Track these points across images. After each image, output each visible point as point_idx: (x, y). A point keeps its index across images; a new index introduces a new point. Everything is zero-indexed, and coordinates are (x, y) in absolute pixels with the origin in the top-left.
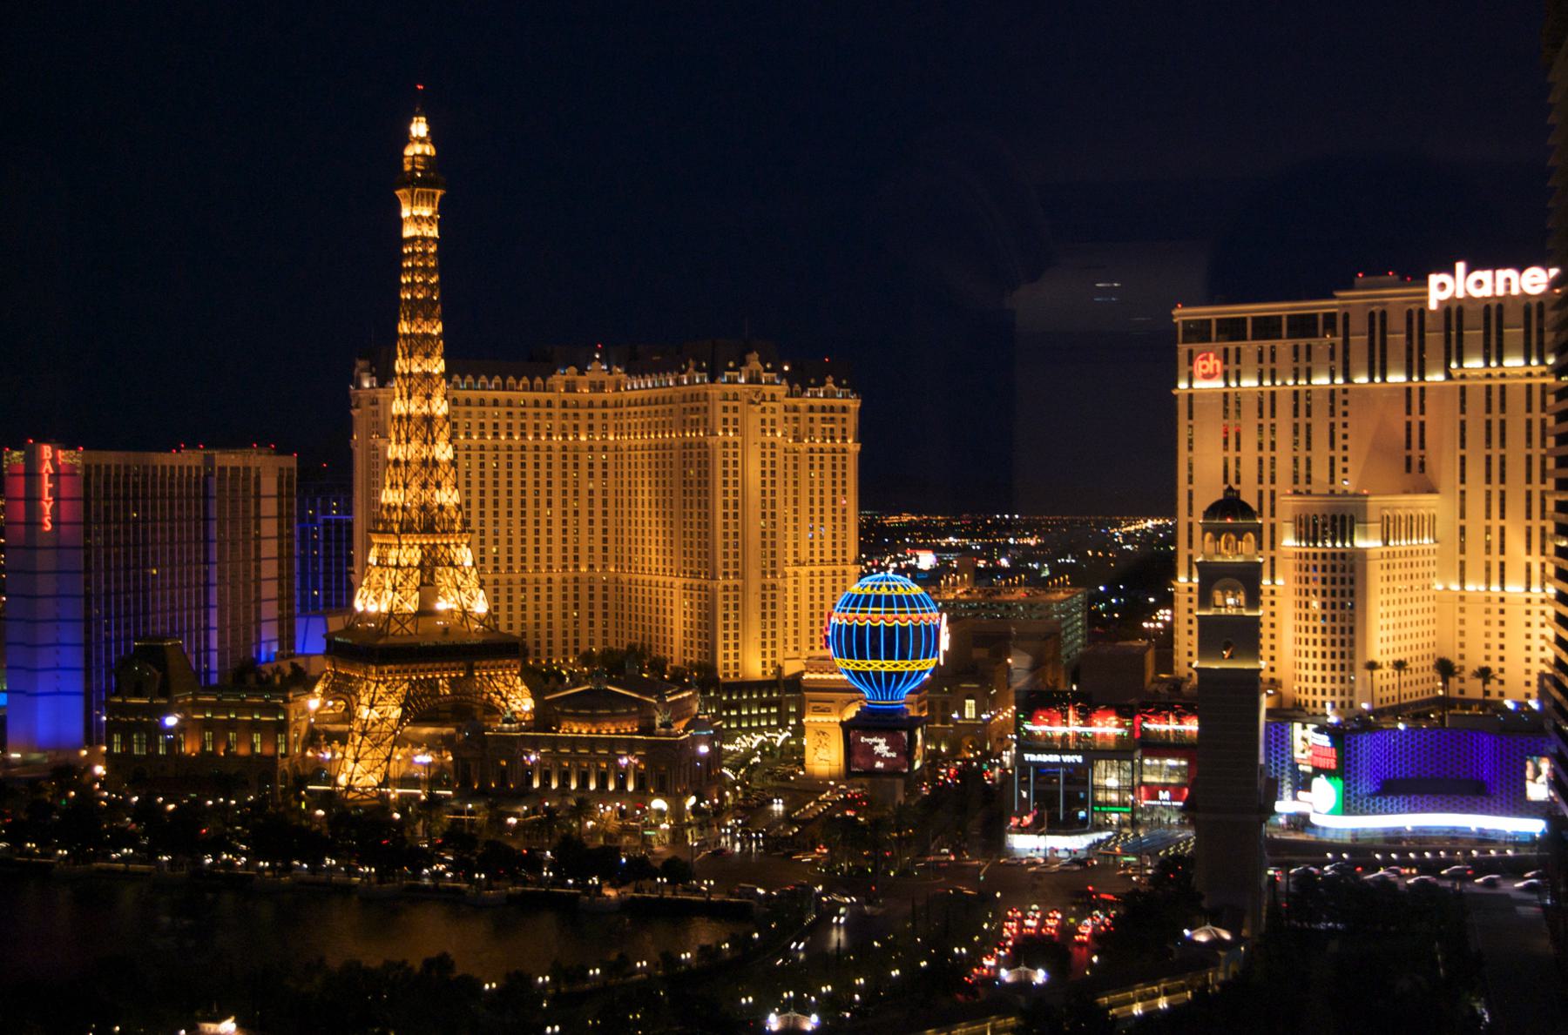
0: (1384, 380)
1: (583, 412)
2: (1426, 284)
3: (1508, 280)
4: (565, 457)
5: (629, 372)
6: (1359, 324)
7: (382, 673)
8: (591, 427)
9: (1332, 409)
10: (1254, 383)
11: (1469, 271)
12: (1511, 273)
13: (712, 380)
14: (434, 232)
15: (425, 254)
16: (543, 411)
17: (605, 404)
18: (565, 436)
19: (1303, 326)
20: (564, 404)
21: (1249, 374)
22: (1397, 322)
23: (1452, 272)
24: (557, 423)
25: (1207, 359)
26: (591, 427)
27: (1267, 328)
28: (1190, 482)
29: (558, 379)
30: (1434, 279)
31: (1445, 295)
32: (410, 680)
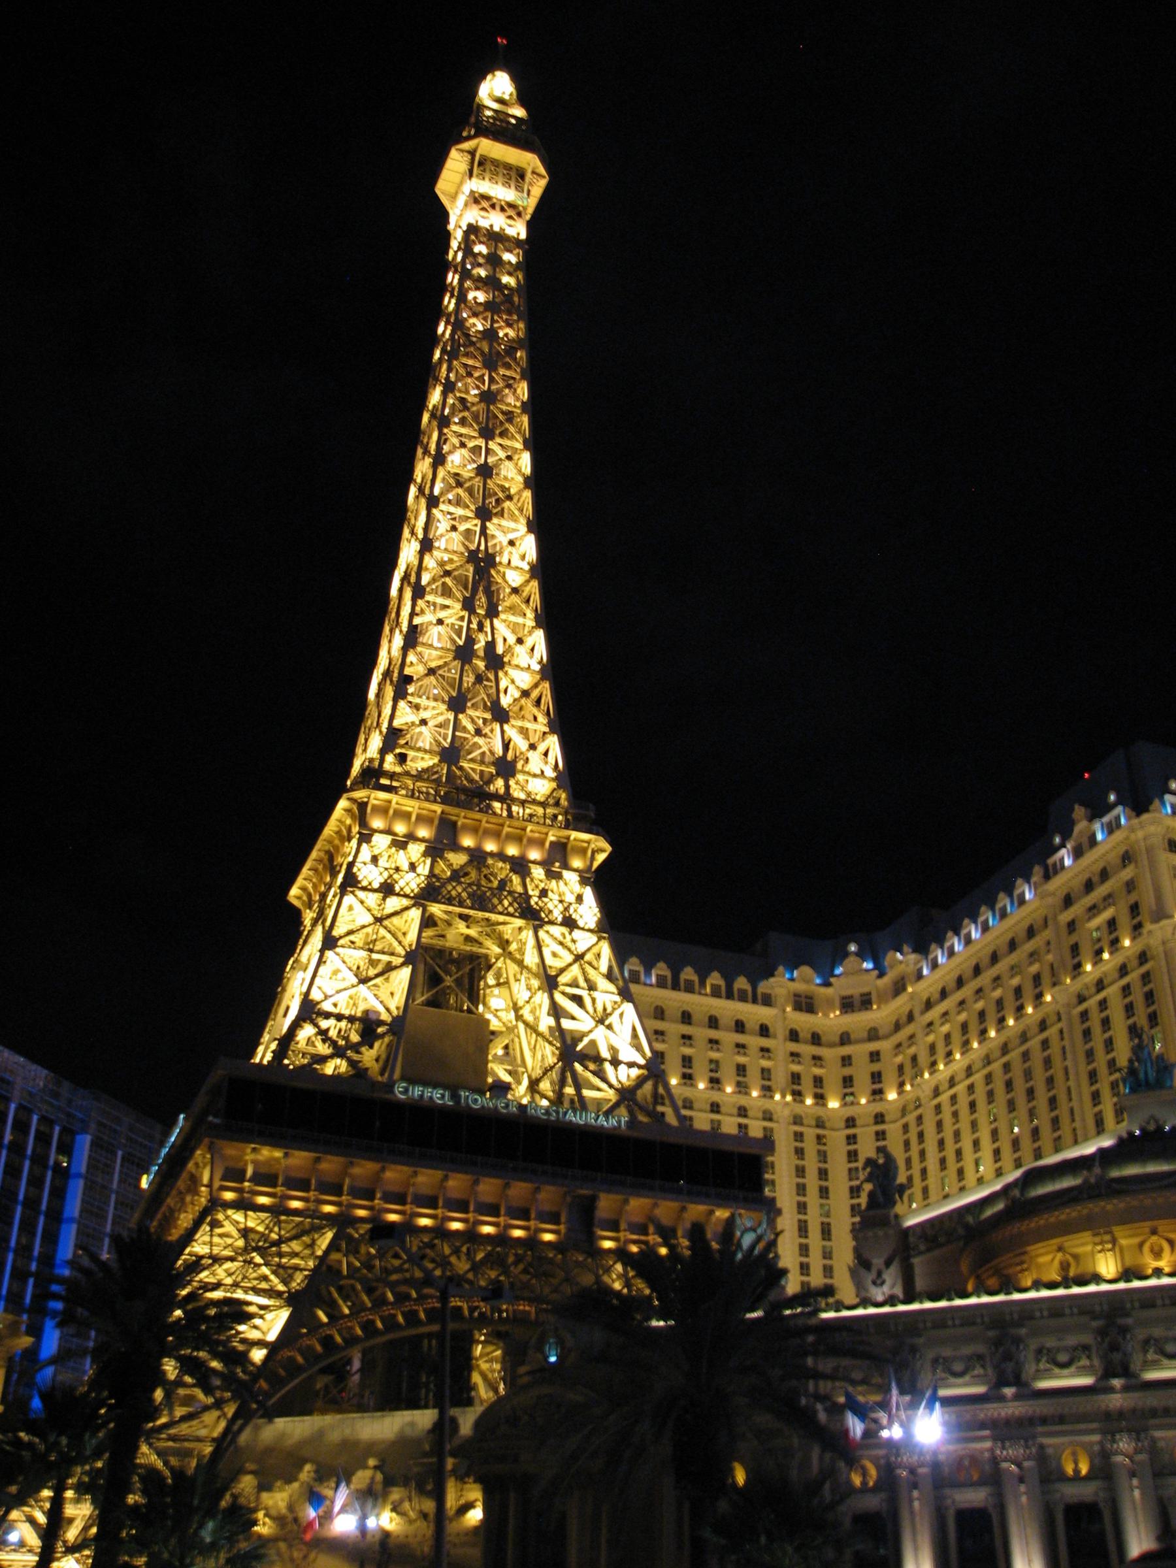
1: (831, 1054)
4: (799, 1136)
5: (922, 949)
7: (235, 1174)
8: (848, 1081)
13: (1140, 807)
14: (519, 230)
15: (494, 260)
16: (754, 1042)
17: (873, 1035)
18: (798, 1095)
20: (794, 1036)
24: (781, 1070)
26: (848, 1081)
29: (782, 983)
32: (342, 1222)
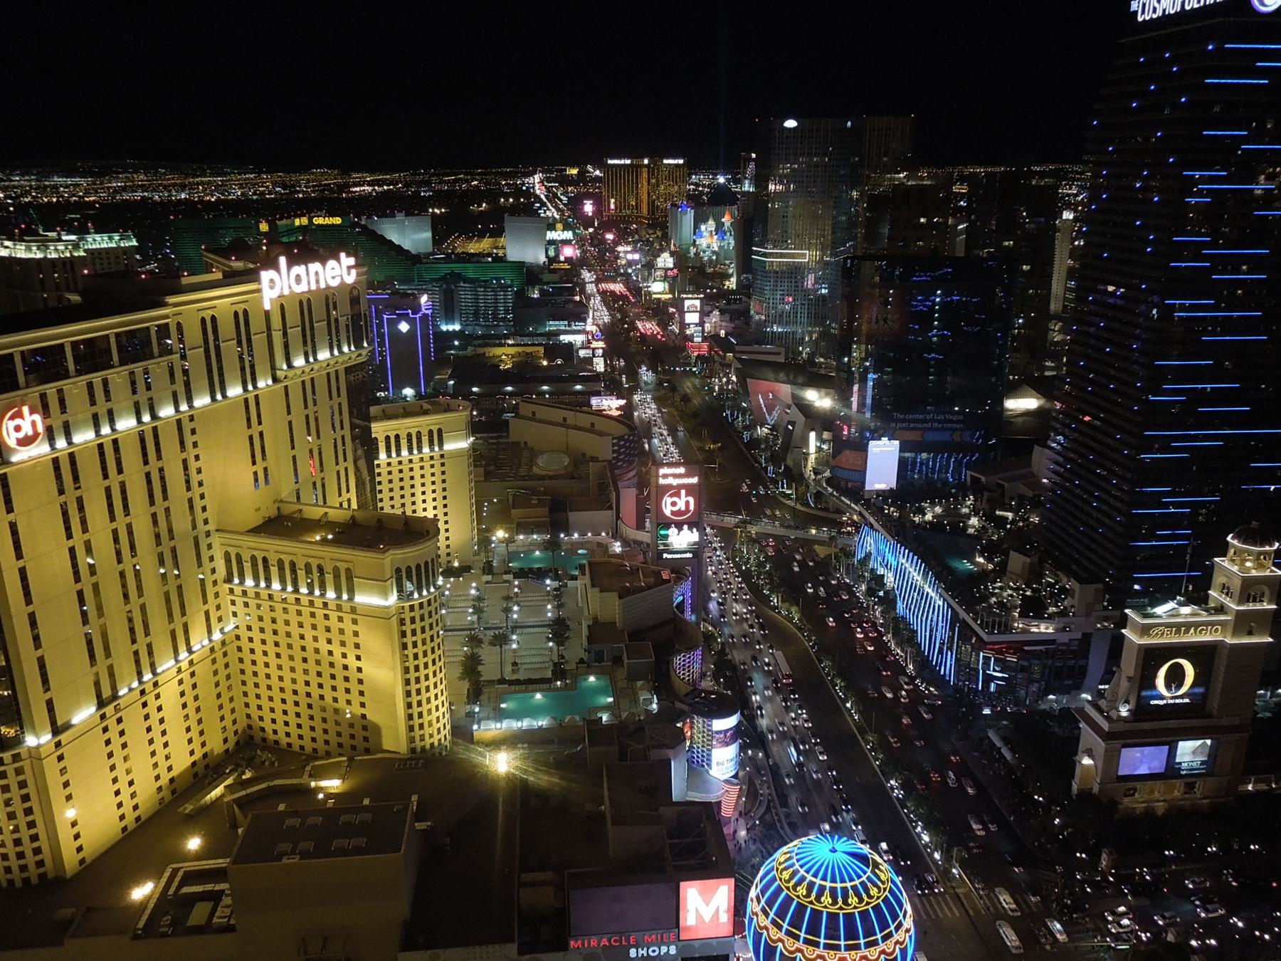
0: (224, 396)
2: (257, 280)
3: (317, 273)
6: (193, 334)
9: (182, 443)
10: (89, 435)
11: (289, 266)
12: (315, 267)
19: (136, 348)
21: (81, 425)
22: (227, 328)
23: (277, 269)
25: (22, 417)
27: (93, 356)
28: (28, 601)
30: (266, 275)
31: (275, 294)
